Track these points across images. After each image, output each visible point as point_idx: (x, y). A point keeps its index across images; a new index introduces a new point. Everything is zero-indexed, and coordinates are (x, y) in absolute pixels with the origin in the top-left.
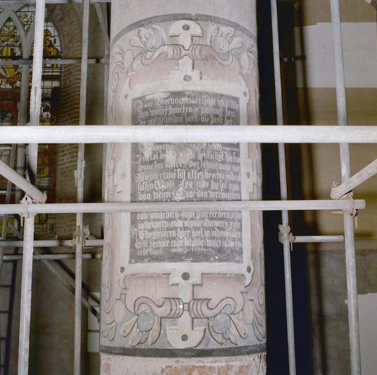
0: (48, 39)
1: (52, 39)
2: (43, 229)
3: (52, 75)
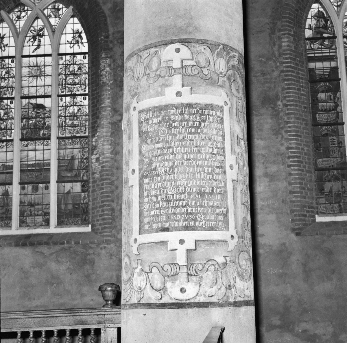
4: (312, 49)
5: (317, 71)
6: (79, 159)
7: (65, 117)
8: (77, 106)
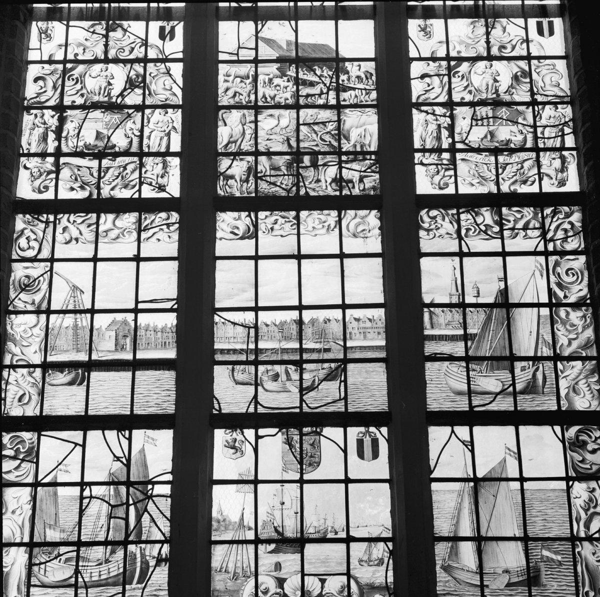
6: (539, 305)
7: (450, 105)
8: (509, 59)
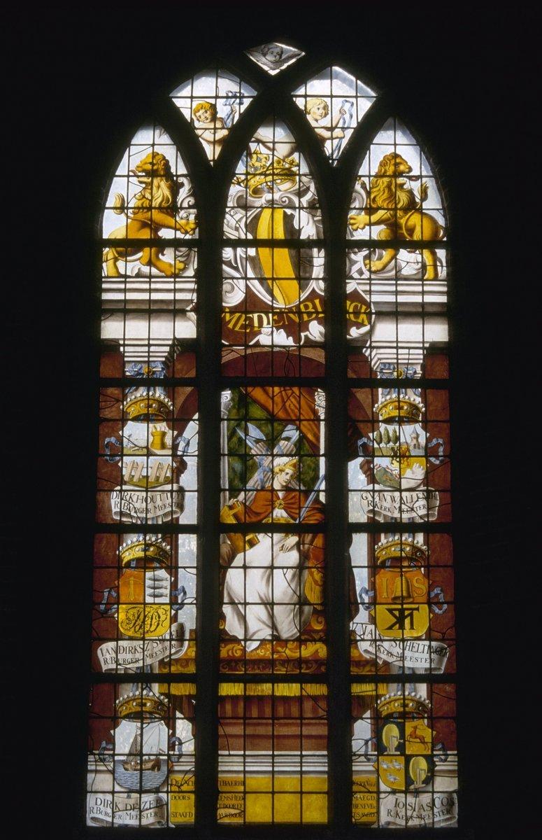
0: (402, 185)
1: (415, 186)
2: (422, 807)
3: (423, 305)
4: (121, 276)
5: (127, 349)
